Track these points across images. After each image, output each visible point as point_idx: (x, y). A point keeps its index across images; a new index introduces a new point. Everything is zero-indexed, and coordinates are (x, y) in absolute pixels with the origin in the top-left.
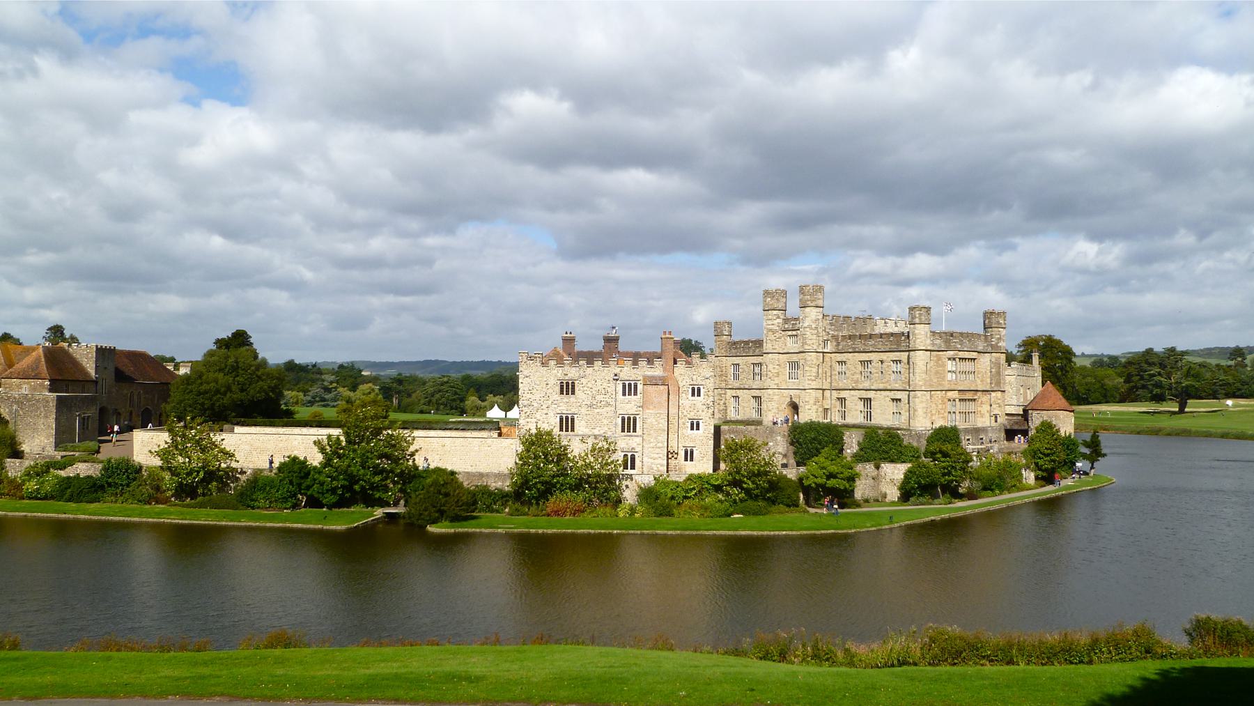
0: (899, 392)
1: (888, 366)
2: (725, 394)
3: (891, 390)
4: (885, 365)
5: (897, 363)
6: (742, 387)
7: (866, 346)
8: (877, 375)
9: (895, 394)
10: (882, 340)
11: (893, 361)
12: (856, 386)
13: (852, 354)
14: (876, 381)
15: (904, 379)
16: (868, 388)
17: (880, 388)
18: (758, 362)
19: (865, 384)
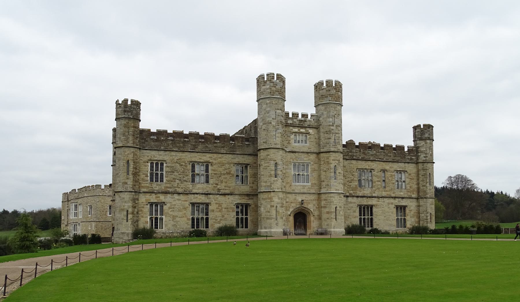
0: (404, 199)
1: (391, 176)
2: (138, 199)
3: (395, 198)
4: (388, 174)
5: (401, 173)
6: (170, 190)
7: (366, 155)
8: (380, 183)
9: (399, 201)
10: (385, 151)
11: (397, 171)
12: (354, 193)
13: (348, 162)
14: (379, 189)
15: (409, 188)
16: (369, 195)
17: (383, 195)
18: (202, 161)
19: (365, 192)
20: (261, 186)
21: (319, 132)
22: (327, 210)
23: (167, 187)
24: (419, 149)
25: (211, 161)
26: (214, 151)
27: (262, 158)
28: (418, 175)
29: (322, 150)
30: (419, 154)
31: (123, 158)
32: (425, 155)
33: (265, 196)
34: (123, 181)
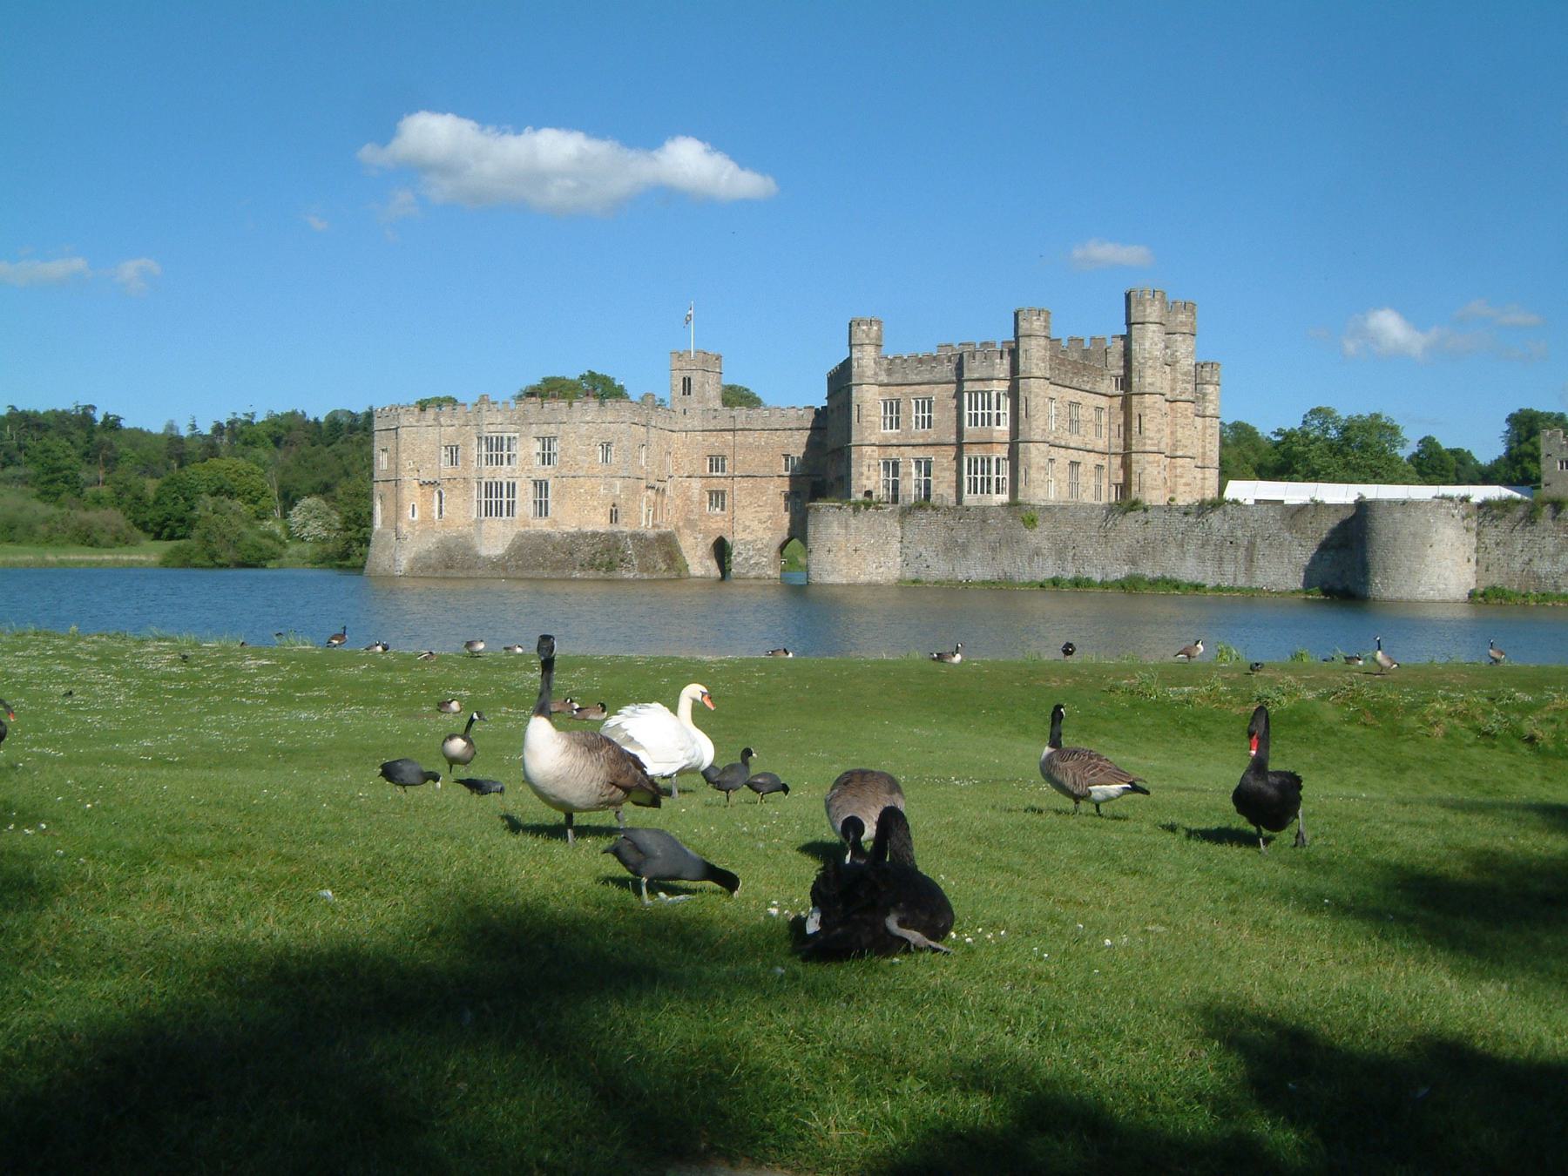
6: (1057, 442)
20: (1145, 444)
21: (1174, 371)
22: (1183, 481)
23: (1055, 438)
24: (1207, 397)
25: (1081, 402)
26: (1083, 387)
27: (1147, 405)
28: (1204, 434)
29: (1179, 398)
30: (1207, 404)
31: (1042, 393)
32: (1214, 407)
33: (1151, 457)
34: (1043, 427)
